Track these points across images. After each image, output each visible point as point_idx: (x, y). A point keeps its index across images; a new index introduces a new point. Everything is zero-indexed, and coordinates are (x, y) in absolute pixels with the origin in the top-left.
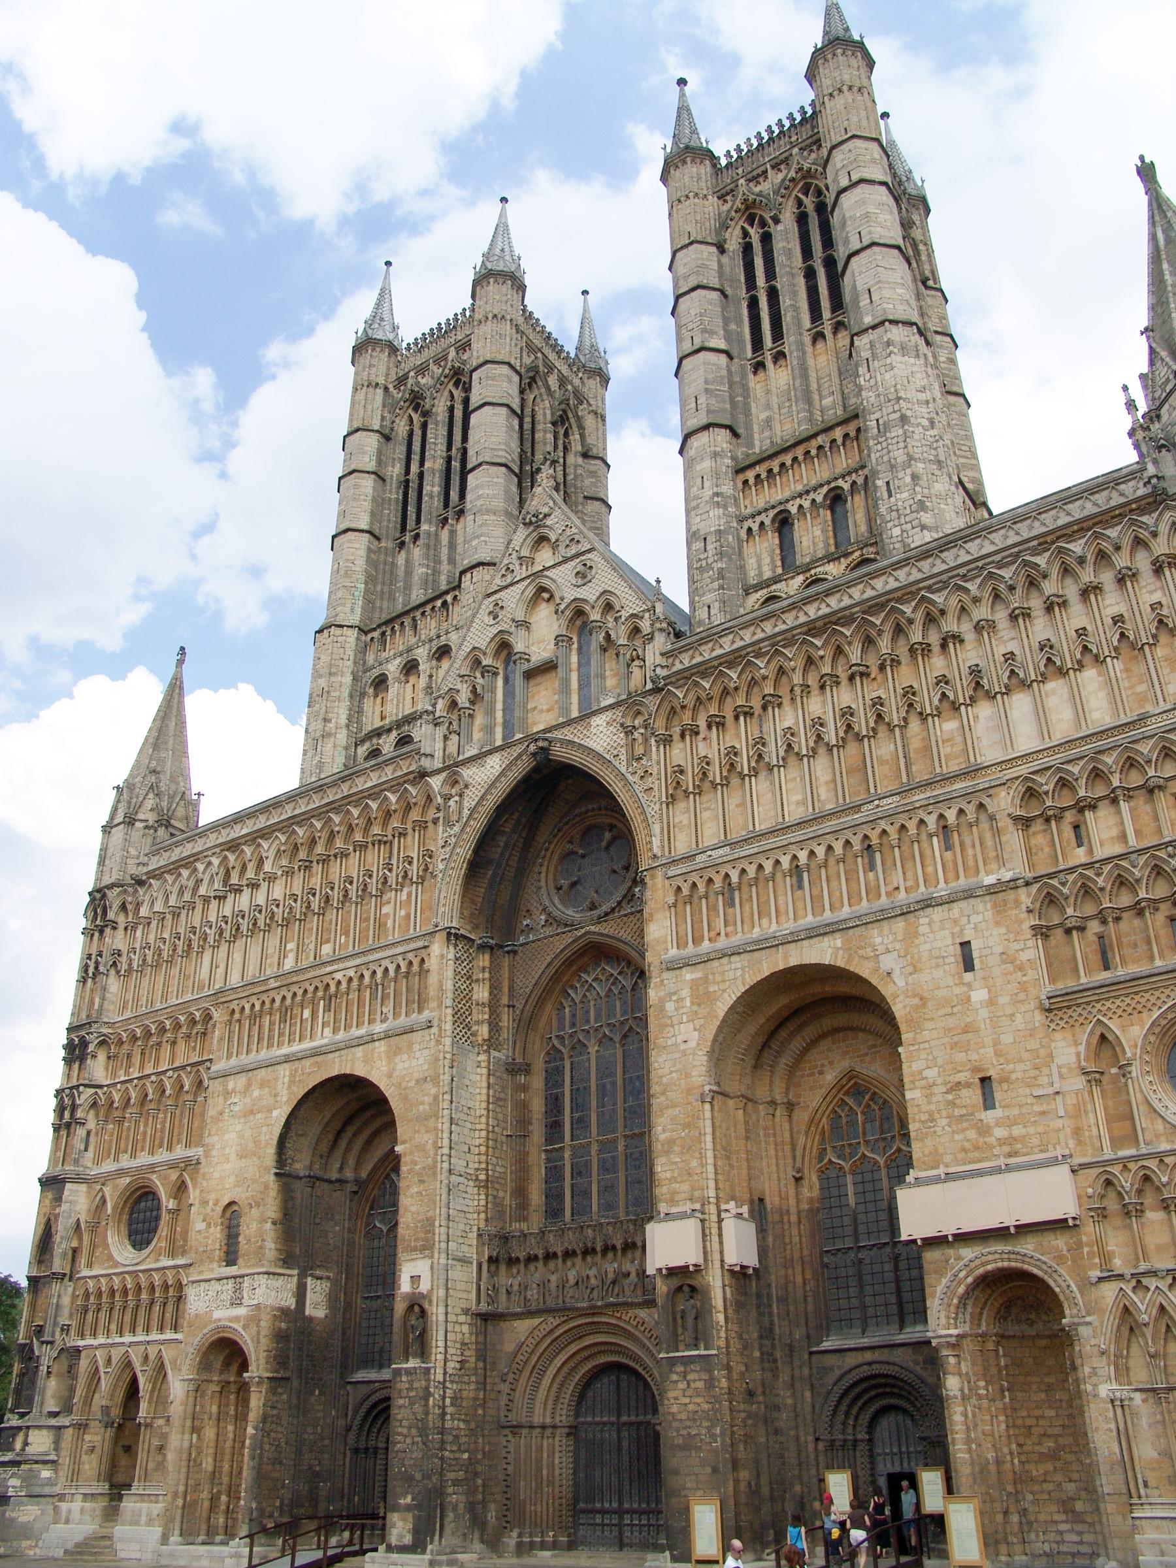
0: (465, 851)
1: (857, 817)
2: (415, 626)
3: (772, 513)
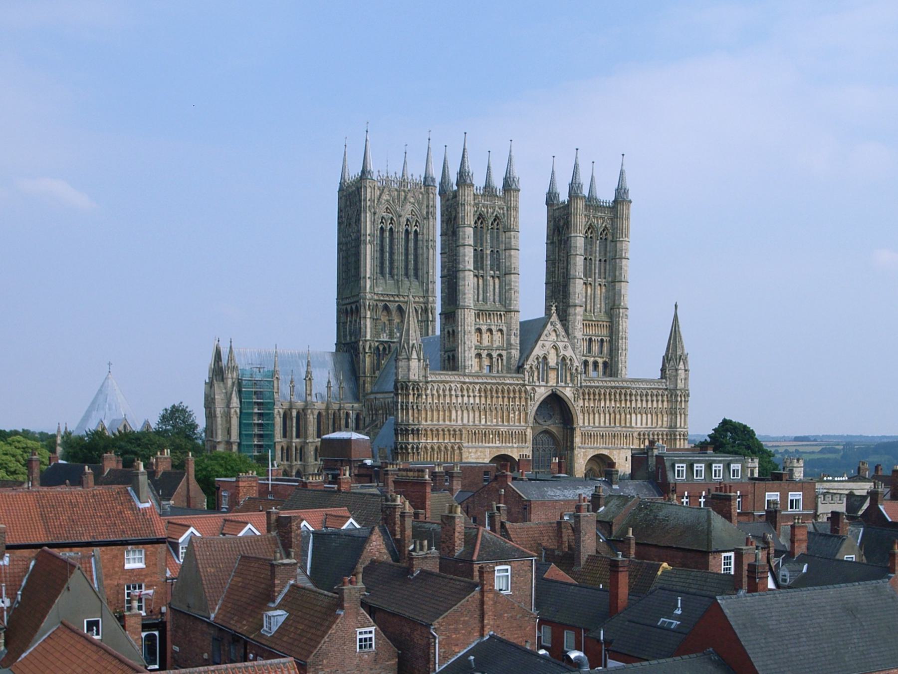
0: (535, 408)
1: (614, 429)
2: (490, 314)
3: (589, 337)
